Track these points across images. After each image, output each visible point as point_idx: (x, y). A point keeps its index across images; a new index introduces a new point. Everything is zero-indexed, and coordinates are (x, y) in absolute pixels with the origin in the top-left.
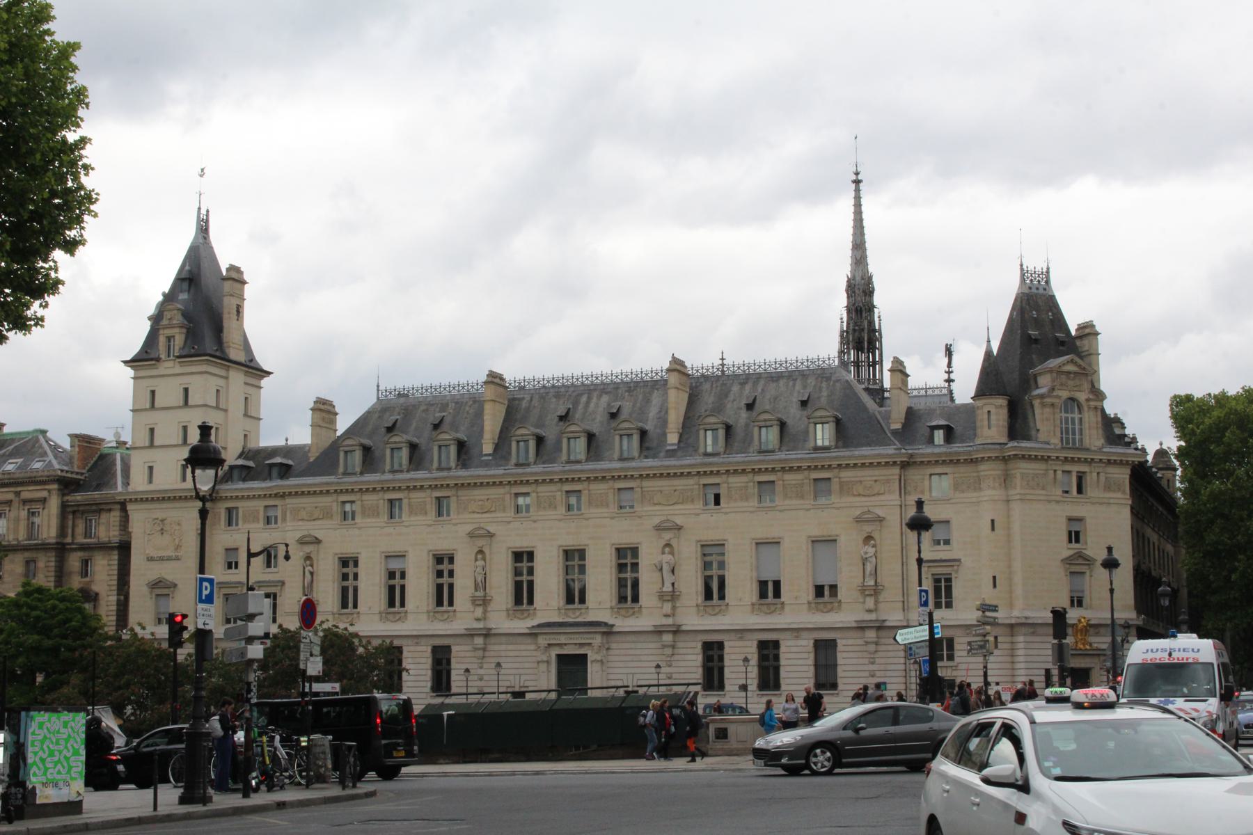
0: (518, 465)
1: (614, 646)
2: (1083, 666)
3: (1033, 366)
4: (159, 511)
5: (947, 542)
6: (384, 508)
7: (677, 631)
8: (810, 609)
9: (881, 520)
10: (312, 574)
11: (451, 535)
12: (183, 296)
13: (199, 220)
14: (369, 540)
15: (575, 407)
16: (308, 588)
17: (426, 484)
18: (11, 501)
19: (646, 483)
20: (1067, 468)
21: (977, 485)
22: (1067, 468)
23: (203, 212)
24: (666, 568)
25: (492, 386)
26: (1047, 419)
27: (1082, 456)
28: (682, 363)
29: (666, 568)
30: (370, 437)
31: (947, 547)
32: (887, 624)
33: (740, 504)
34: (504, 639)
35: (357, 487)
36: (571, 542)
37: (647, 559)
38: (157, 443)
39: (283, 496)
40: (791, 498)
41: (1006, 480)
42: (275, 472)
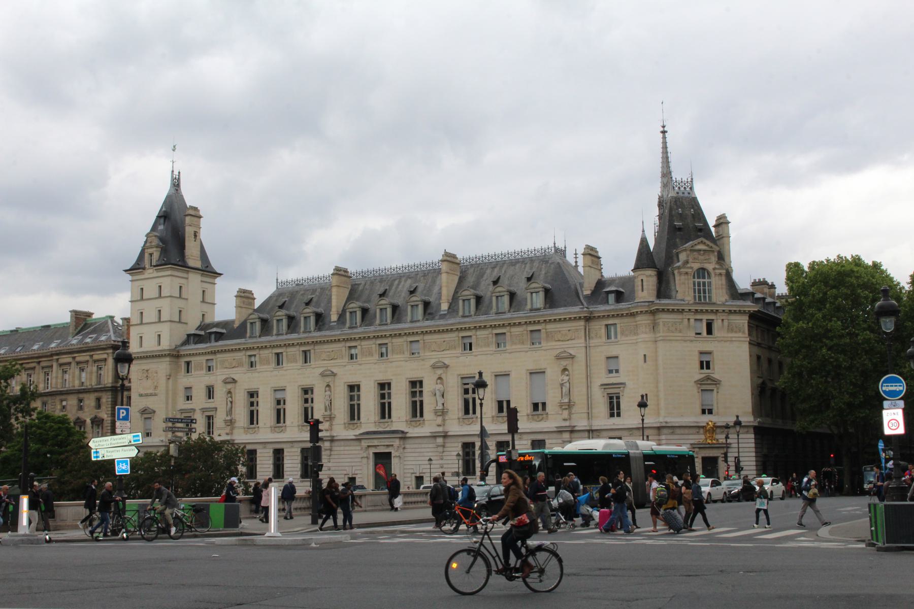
0: (350, 328)
1: (407, 446)
2: (711, 455)
3: (676, 247)
5: (617, 371)
6: (273, 359)
7: (445, 436)
8: (528, 419)
9: (572, 357)
10: (231, 402)
11: (311, 375)
12: (161, 227)
13: (173, 179)
14: (265, 379)
15: (390, 289)
16: (230, 412)
17: (295, 342)
18: (88, 361)
19: (427, 337)
20: (699, 317)
21: (635, 331)
22: (699, 317)
23: (176, 173)
24: (438, 393)
25: (336, 277)
26: (684, 284)
27: (709, 308)
28: (454, 256)
29: (438, 393)
30: (268, 313)
31: (617, 375)
32: (576, 428)
33: (484, 349)
34: (342, 443)
35: (256, 346)
36: (383, 378)
37: (427, 388)
38: (144, 321)
39: (214, 353)
40: (515, 344)
41: (654, 327)
42: (213, 336)
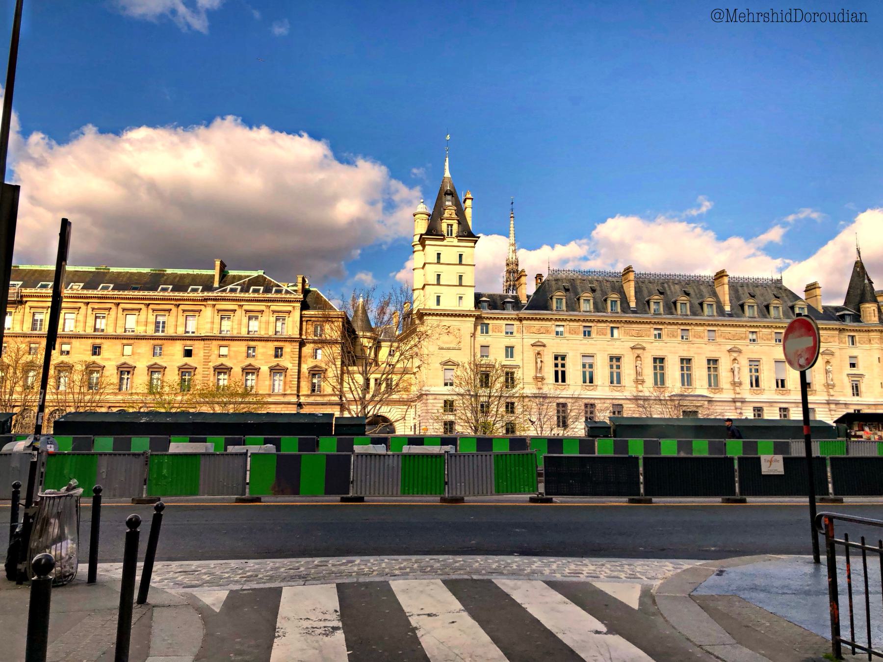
4: (447, 321)
36: (686, 355)
